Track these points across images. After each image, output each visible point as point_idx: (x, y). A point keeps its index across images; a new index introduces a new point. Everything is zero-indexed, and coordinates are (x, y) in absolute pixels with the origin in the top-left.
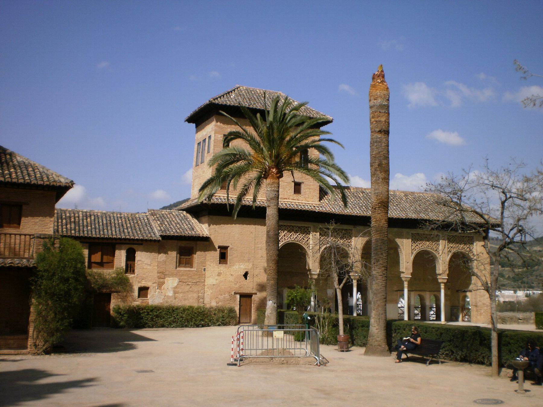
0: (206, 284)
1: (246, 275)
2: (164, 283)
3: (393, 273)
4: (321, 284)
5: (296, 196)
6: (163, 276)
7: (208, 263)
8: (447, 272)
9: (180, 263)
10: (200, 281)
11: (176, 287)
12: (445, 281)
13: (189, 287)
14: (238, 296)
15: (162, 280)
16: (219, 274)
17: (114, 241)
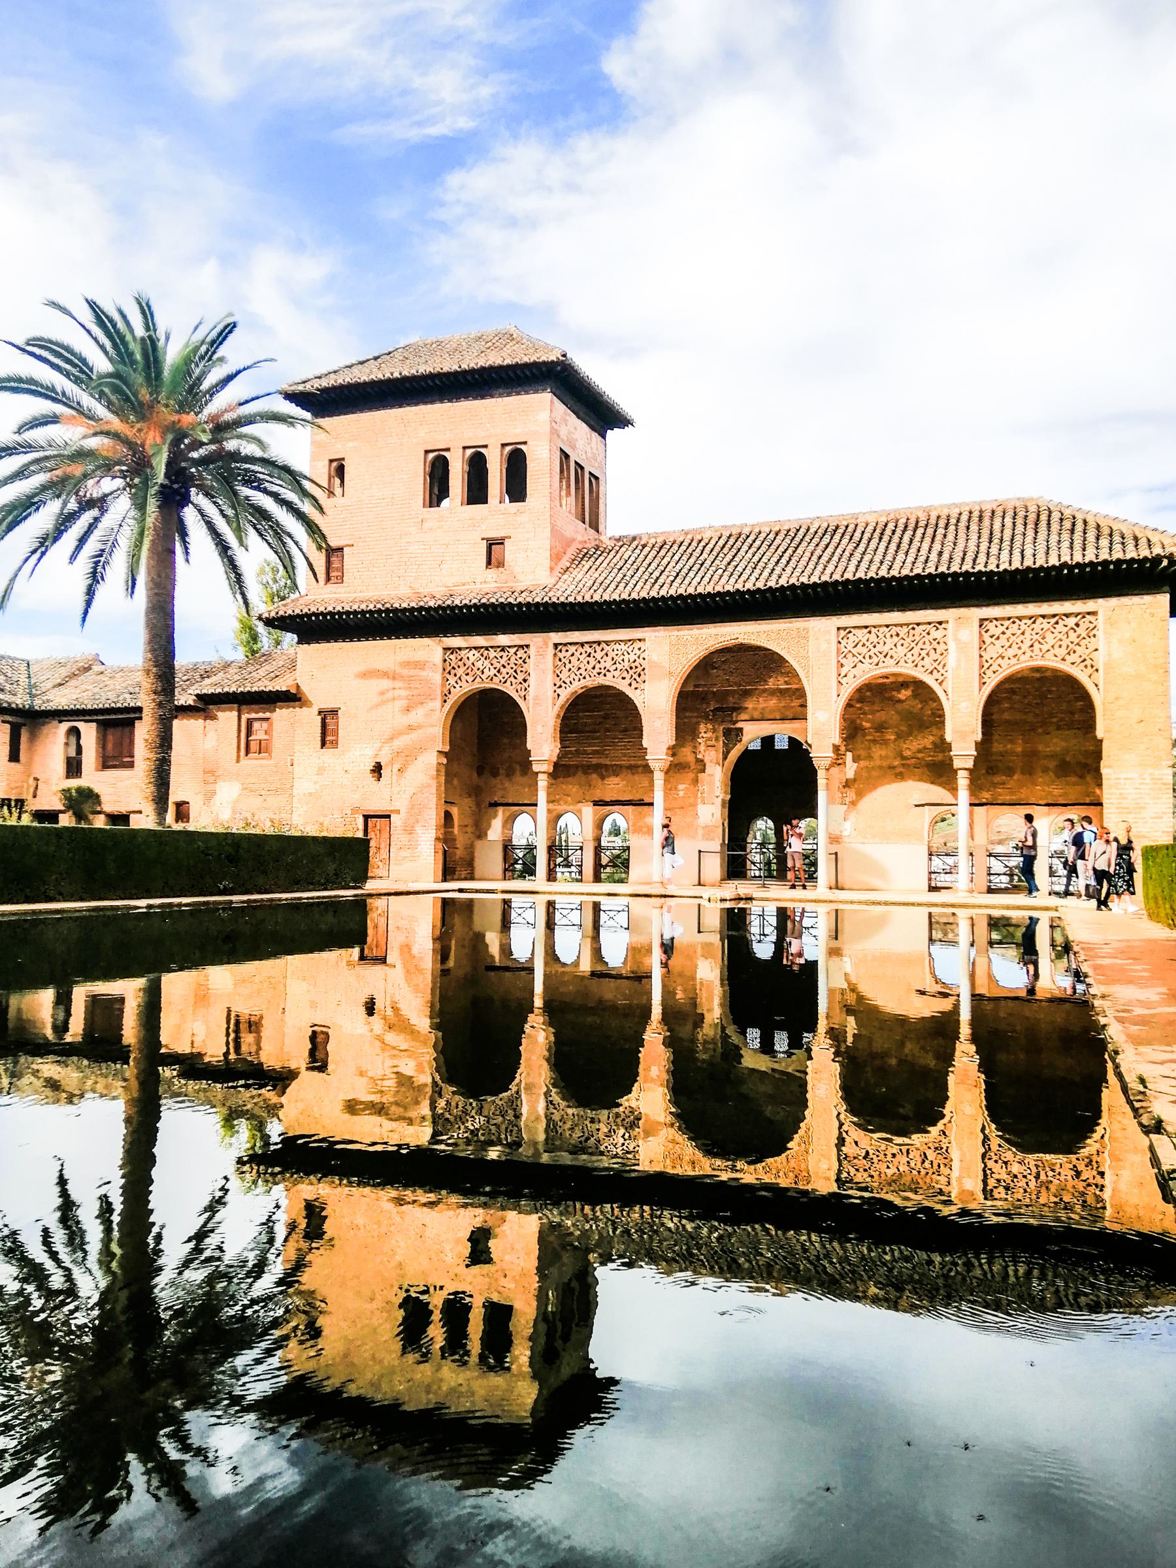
0: (295, 792)
1: (377, 769)
2: (214, 793)
3: (907, 753)
4: (681, 794)
5: (492, 573)
6: (211, 779)
7: (297, 748)
8: (979, 737)
9: (247, 752)
10: (285, 788)
11: (237, 801)
12: (970, 764)
13: (261, 799)
14: (361, 820)
15: (211, 787)
16: (321, 771)
17: (133, 716)
